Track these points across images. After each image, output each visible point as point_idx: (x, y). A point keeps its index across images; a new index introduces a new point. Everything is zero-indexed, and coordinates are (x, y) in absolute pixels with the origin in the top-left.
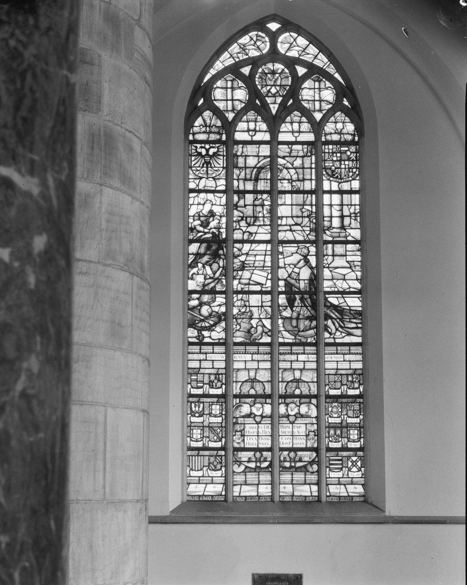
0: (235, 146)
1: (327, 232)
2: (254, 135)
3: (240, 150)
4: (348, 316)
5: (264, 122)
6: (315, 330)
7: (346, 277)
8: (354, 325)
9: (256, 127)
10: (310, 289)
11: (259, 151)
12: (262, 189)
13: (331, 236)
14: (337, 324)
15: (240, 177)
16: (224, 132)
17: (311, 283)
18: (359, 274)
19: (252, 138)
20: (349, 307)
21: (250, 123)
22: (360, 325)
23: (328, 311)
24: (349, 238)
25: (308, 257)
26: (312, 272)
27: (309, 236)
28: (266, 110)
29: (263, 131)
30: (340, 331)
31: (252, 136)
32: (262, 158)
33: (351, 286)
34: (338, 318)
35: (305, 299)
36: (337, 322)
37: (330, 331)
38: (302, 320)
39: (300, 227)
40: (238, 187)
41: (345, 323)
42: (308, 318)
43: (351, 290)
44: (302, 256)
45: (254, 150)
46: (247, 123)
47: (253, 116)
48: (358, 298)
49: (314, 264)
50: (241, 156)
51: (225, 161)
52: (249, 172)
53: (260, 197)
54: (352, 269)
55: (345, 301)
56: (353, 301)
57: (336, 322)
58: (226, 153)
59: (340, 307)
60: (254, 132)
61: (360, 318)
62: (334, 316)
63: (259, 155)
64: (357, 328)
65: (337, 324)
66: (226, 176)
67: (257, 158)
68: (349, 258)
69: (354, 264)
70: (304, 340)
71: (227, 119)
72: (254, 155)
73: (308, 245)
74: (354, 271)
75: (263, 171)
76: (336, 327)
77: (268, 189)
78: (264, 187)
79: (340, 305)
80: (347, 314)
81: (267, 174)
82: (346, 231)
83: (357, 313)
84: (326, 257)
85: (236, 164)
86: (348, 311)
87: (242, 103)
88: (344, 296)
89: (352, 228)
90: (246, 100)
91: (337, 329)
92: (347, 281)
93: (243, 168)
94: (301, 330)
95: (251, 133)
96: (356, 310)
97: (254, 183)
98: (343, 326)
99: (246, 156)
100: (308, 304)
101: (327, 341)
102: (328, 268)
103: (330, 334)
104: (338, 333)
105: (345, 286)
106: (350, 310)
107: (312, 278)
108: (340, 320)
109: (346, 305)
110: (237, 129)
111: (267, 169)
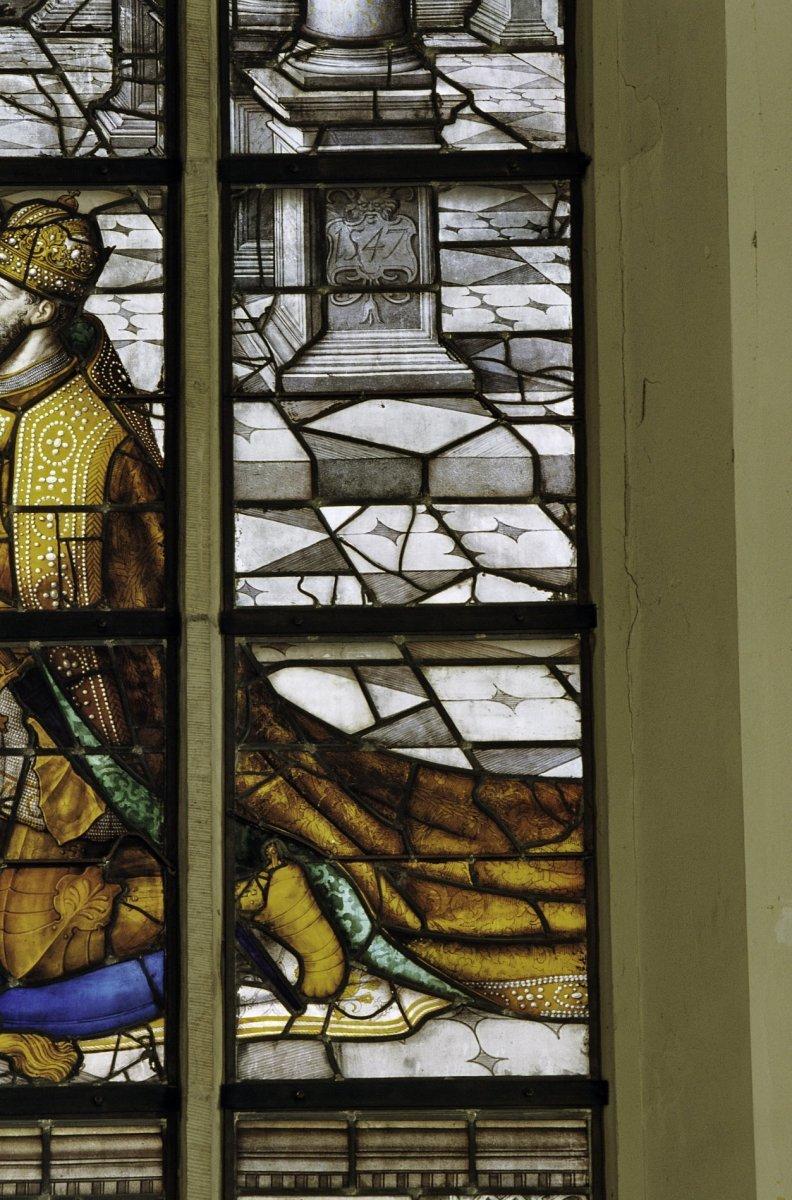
1: (260, 77)
4: (457, 834)
6: (156, 963)
7: (448, 476)
8: (503, 918)
10: (109, 586)
13: (298, 115)
14: (350, 905)
17: (121, 534)
18: (557, 443)
20: (475, 749)
22: (566, 919)
23: (274, 793)
24: (464, 135)
25: (96, 305)
26: (131, 436)
27: (111, 122)
30: (379, 974)
33: (484, 561)
34: (369, 854)
35: (68, 684)
36: (357, 886)
37: (290, 970)
38: (31, 880)
39: (24, 37)
41: (433, 891)
42: (84, 855)
43: (495, 591)
44: (38, 295)
48: (551, 665)
49: (145, 368)
54: (489, 407)
55: (434, 701)
56: (501, 697)
57: (345, 893)
59: (384, 751)
61: (572, 846)
62: (323, 833)
64: (545, 940)
65: (350, 905)
68: (465, 312)
69: (507, 362)
70: (42, 1061)
73: (87, 202)
74: (508, 423)
76: (342, 936)
79: (377, 734)
80: (445, 813)
82: (436, 75)
83: (545, 811)
84: (258, 305)
86: (462, 789)
88: (428, 651)
89: (487, 48)
91: (353, 955)
92: (454, 516)
94: (25, 965)
96: (530, 781)
98: (411, 919)
100: (92, 727)
101: (258, 1065)
102: (277, 398)
103: (294, 998)
104: (366, 1000)
105: (430, 552)
106: (477, 775)
107: (126, 495)
108: (389, 866)
109: (444, 730)
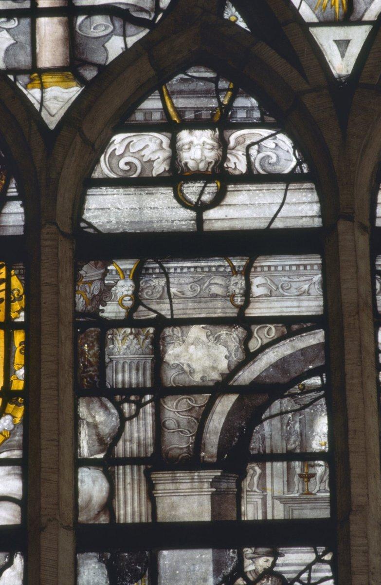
0: (89, 272)
2: (217, 200)
3: (124, 288)
5: (280, 125)
9: (224, 158)
11: (247, 293)
12: (278, 513)
15: (121, 449)
16: (13, 191)
19: (200, 221)
21: (185, 136)
28: (293, 59)
29: (272, 178)
31: (200, 208)
32: (273, 331)
40: (109, 506)
45: (215, 289)
46: (164, 139)
47: (206, 93)
50: (130, 321)
51: (19, 358)
52: (184, 419)
53: (263, 563)
58: (26, 309)
60: (212, 188)
63: (255, 310)
66: (25, 446)
67: (238, 333)
71: (33, 115)
72: (219, 314)
75: (276, 406)
77: (324, 513)
78: (284, 501)
81: (309, 425)
85: (91, 370)
87: (131, 29)
90: (157, 9)
93: (140, 391)
95: (191, 190)
97: (215, 482)
99: (161, 323)
110: (103, 169)
111: (307, 398)
